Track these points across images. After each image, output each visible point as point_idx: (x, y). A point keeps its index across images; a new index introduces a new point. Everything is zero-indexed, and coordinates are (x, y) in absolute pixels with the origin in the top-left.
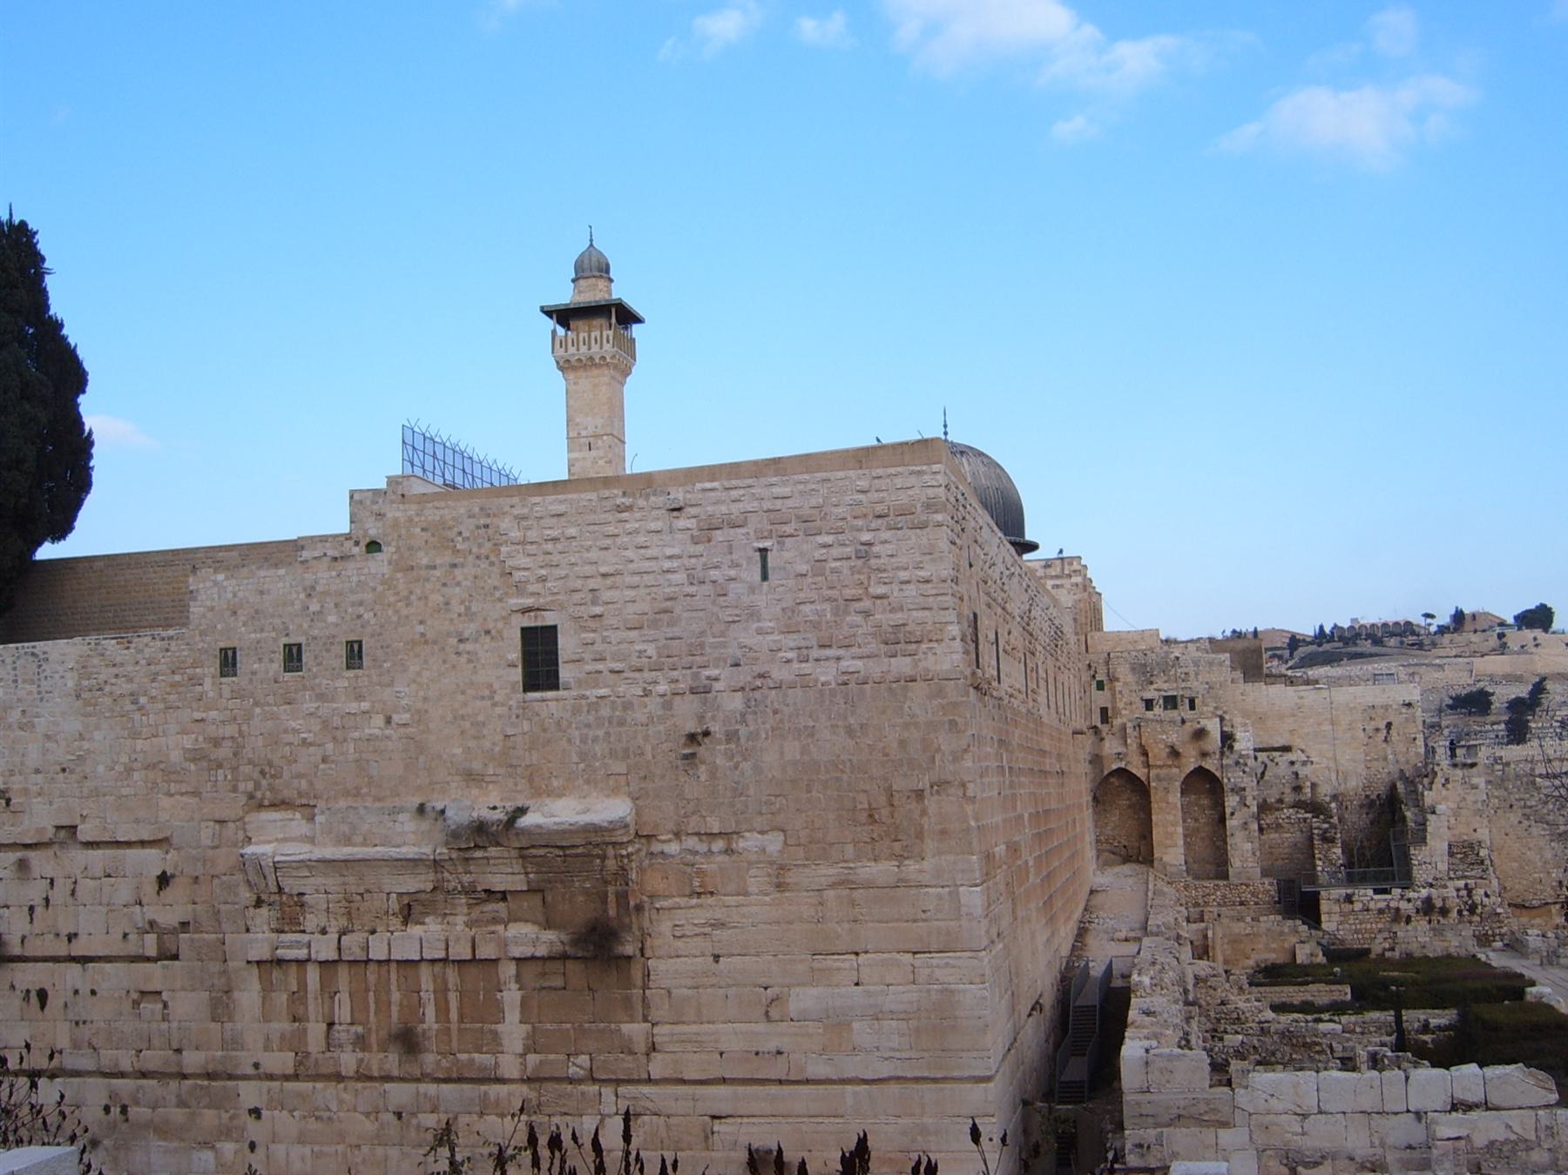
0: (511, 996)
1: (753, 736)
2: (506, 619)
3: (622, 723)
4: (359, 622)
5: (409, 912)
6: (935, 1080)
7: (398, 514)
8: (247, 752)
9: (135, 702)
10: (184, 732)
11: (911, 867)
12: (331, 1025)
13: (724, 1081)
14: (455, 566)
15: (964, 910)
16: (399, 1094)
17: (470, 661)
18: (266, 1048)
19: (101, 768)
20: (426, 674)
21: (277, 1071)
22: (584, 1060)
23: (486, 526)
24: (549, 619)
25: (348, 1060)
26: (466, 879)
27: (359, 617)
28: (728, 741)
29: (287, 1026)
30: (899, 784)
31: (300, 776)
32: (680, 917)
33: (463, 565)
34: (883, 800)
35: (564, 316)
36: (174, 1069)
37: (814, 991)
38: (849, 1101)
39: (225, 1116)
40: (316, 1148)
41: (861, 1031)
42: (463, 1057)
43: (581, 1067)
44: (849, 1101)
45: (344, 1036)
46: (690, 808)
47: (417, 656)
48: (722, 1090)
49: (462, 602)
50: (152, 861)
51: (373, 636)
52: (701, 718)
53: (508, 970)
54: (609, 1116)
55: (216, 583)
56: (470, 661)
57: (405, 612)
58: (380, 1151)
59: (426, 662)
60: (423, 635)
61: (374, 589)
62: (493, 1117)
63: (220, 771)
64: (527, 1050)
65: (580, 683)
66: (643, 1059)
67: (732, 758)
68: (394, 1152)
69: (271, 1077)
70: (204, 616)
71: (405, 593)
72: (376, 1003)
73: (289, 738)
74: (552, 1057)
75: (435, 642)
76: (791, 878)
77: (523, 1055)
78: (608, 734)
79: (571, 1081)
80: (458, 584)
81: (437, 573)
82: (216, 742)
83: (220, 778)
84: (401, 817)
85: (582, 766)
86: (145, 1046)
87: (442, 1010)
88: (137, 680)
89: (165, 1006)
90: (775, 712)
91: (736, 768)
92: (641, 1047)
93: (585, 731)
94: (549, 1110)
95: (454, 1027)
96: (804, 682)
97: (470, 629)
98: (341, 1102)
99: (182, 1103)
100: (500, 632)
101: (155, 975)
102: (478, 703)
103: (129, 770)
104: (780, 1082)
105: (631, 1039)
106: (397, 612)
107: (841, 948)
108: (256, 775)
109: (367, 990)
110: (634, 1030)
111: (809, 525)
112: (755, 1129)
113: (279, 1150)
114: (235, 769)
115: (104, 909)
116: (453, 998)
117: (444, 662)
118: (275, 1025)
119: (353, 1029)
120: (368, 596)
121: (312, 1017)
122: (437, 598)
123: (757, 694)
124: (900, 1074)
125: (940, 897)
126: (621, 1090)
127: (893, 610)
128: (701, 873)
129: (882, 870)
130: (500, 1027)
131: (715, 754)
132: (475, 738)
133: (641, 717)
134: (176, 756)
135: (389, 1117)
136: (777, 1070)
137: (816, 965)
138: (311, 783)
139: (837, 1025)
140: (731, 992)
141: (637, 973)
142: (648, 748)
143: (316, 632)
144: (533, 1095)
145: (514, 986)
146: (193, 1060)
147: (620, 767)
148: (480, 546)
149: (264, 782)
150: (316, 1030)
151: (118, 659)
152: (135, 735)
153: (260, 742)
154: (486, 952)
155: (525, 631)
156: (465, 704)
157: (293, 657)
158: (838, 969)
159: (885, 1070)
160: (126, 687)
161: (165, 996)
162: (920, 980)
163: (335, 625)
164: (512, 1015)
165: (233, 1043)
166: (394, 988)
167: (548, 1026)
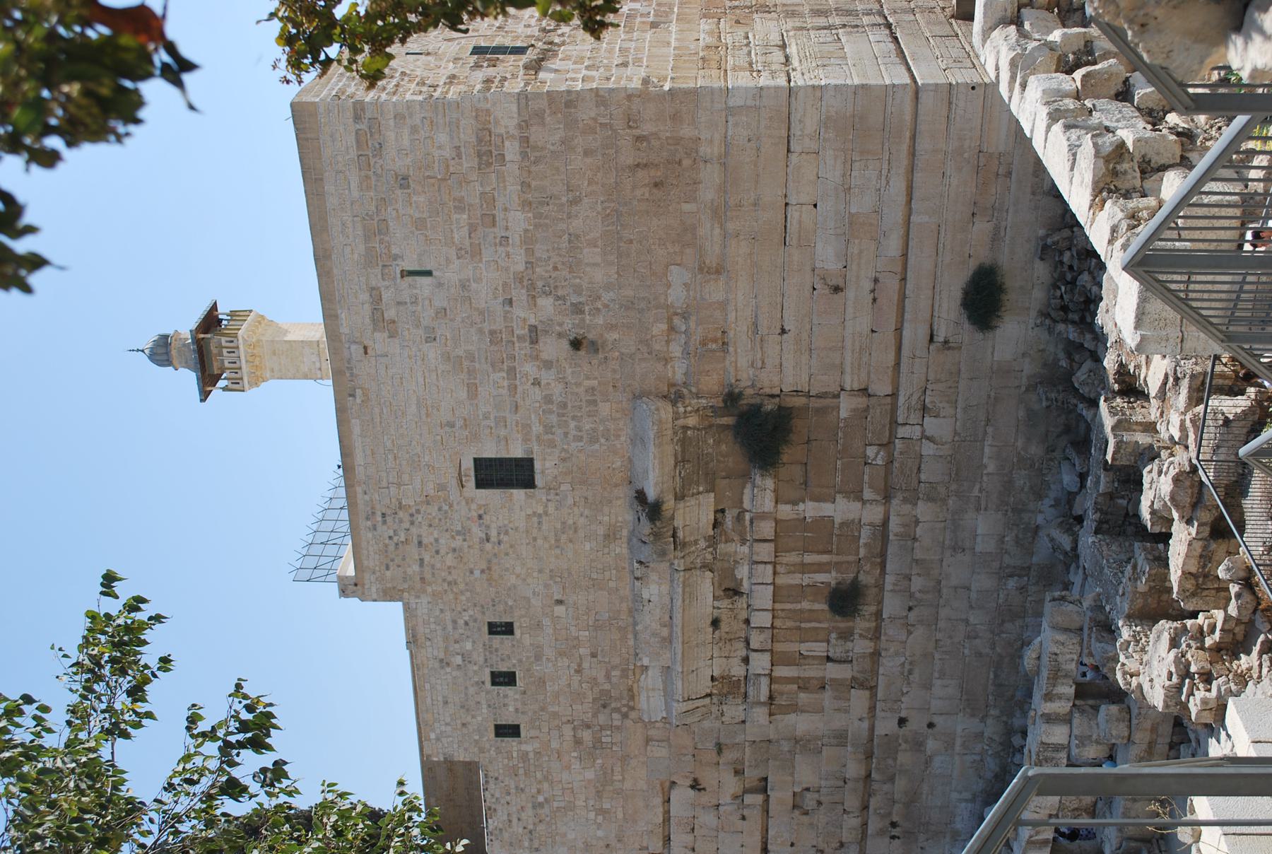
0: (810, 509)
1: (578, 290)
2: (469, 501)
3: (564, 406)
4: (471, 624)
5: (733, 592)
6: (913, 138)
7: (374, 589)
8: (588, 717)
9: (541, 805)
10: (568, 768)
11: (705, 150)
12: (829, 659)
13: (899, 330)
14: (420, 543)
15: (750, 103)
16: (892, 605)
17: (506, 533)
18: (847, 711)
19: (600, 833)
20: (518, 569)
21: (867, 704)
22: (871, 451)
23: (384, 515)
24: (468, 465)
25: (861, 646)
26: (702, 544)
27: (466, 623)
28: (582, 312)
29: (827, 697)
30: (627, 158)
31: (608, 676)
32: (743, 362)
33: (420, 536)
34: (641, 173)
35: (208, 380)
36: (860, 785)
37: (819, 246)
38: (926, 218)
39: (904, 746)
40: (936, 675)
41: (861, 204)
42: (862, 552)
43: (877, 454)
44: (926, 218)
45: (839, 650)
46: (644, 349)
47: (501, 576)
48: (906, 333)
49: (453, 537)
51: (483, 613)
52: (560, 335)
53: (786, 511)
54: (923, 432)
55: (438, 739)
56: (506, 533)
57: (462, 586)
58: (941, 624)
59: (507, 570)
60: (483, 571)
61: (442, 611)
62: (918, 530)
63: (604, 740)
64: (857, 495)
65: (526, 440)
66: (873, 400)
67: (598, 309)
68: (944, 613)
69: (872, 709)
70: (466, 749)
71: (446, 585)
72: (810, 621)
73: (575, 685)
74: (866, 478)
75: (489, 561)
76: (711, 261)
77: (864, 502)
78: (574, 418)
79: (890, 462)
80: (437, 540)
81: (427, 558)
82: (578, 742)
83: (609, 739)
84: (646, 595)
85: (603, 441)
86: (840, 807)
87: (820, 568)
88: (523, 804)
89: (808, 789)
90: (555, 268)
91: (606, 306)
92: (861, 402)
93: (571, 437)
94: (915, 482)
95: (835, 558)
96: (528, 241)
97: (478, 533)
98: (897, 654)
99: (892, 779)
100: (480, 507)
101: (780, 796)
102: (544, 527)
103: (601, 811)
104: (904, 279)
105: (854, 410)
106: (462, 593)
107: (781, 217)
108: (607, 711)
109: (799, 628)
110: (846, 406)
111: (376, 230)
112: (945, 305)
113: (936, 705)
114: (602, 728)
115: (721, 835)
116: (809, 558)
117: (507, 554)
118: (827, 703)
119: (833, 641)
120: (448, 616)
121: (819, 674)
122: (450, 560)
123: (540, 284)
124: (902, 170)
125: (736, 125)
126: (900, 420)
127: (459, 156)
128: (704, 343)
129: (711, 176)
130: (838, 520)
131: (595, 324)
132: (576, 531)
133: (557, 389)
134: (590, 775)
135: (912, 615)
137: (794, 242)
138: (614, 668)
139: (852, 227)
140: (815, 321)
141: (799, 402)
142: (587, 383)
143: (482, 659)
144: (900, 496)
145: (801, 506)
146: (854, 769)
147: (605, 409)
148: (401, 521)
149: (613, 705)
150: (833, 671)
151: (505, 818)
152: (571, 807)
153: (577, 707)
154: (767, 529)
155: (480, 484)
156: (545, 538)
157: (504, 679)
158: (800, 222)
159: (898, 185)
160: (530, 812)
161: (797, 790)
162: (814, 146)
163: (476, 644)
164: (827, 509)
165: (841, 738)
166: (798, 606)
167: (838, 479)
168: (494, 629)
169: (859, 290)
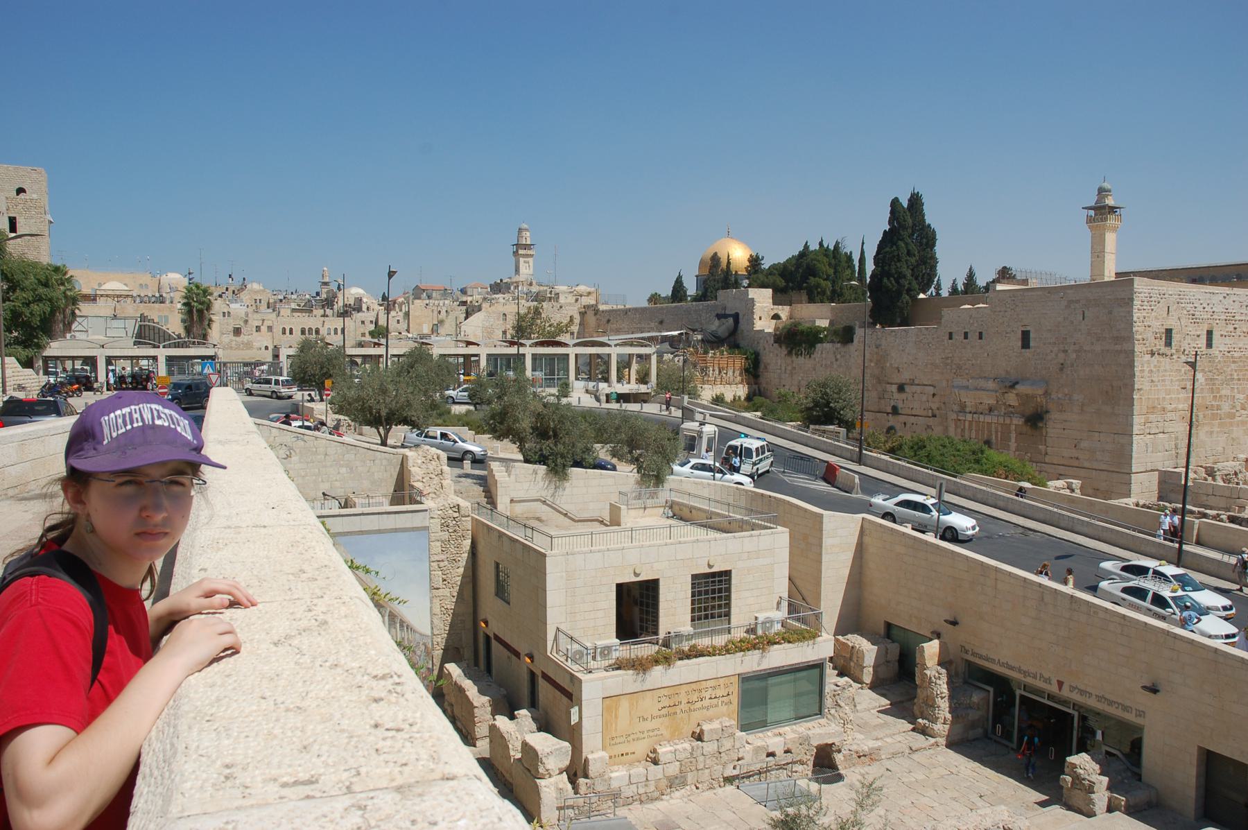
0: (1013, 435)
24: (1028, 328)
50: (931, 390)
101: (931, 421)
136: (1076, 463)
154: (1008, 421)
159: (1104, 467)
164: (1013, 440)
168: (981, 333)
169: (1075, 453)
